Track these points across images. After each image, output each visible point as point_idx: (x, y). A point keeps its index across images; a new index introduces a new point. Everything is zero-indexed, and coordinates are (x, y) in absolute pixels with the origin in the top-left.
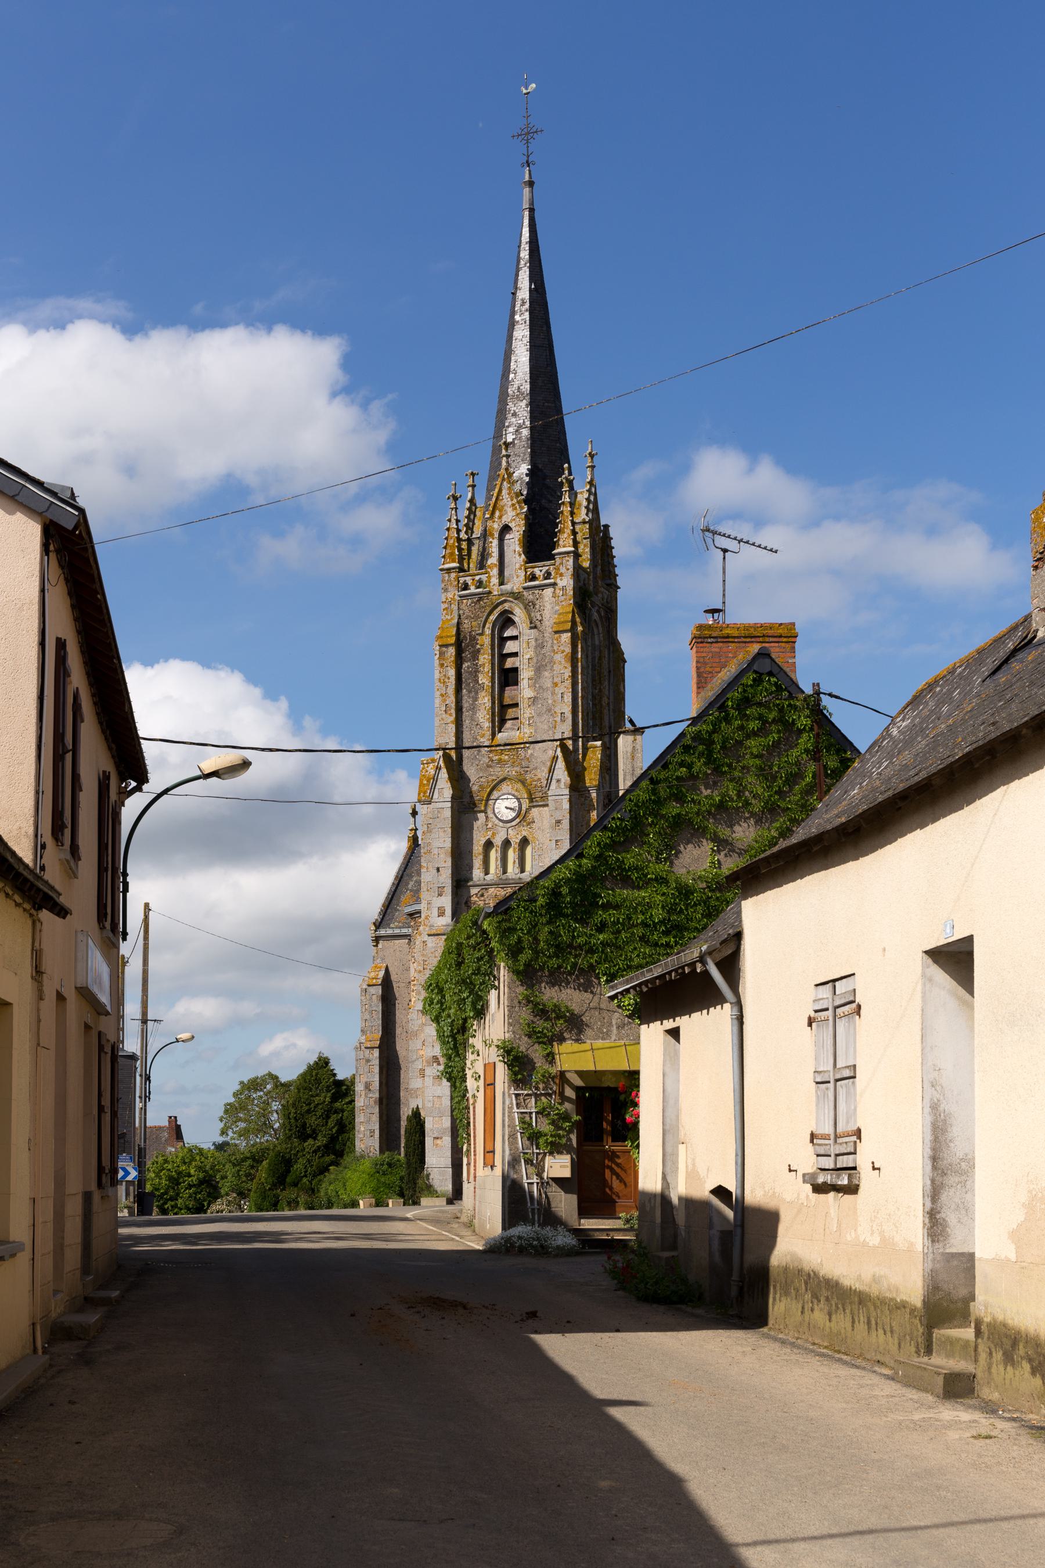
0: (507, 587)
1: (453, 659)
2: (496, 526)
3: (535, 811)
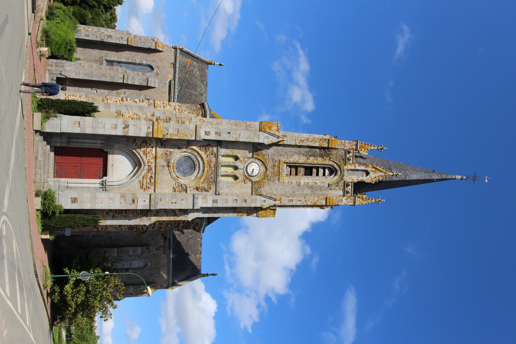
0: (346, 173)
1: (323, 146)
2: (369, 169)
3: (250, 184)
